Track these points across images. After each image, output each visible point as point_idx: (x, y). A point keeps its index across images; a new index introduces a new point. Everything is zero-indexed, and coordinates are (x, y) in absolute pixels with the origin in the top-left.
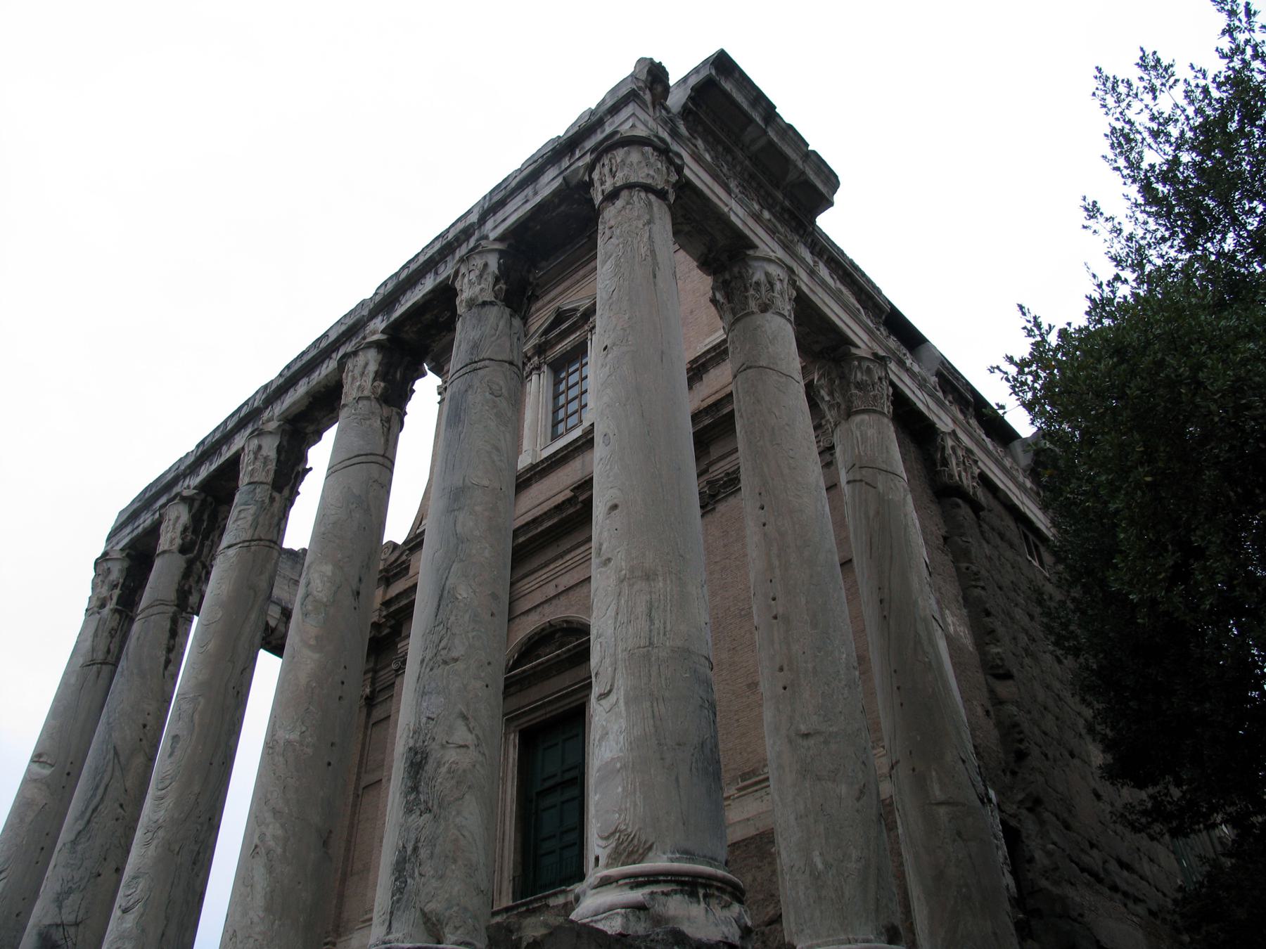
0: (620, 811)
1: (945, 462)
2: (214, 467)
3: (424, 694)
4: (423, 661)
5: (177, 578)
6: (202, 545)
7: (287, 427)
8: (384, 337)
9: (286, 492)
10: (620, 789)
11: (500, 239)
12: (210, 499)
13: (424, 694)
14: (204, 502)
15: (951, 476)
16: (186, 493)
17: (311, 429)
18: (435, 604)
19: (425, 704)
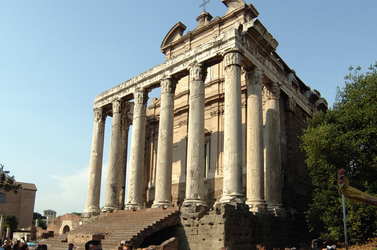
0: (229, 187)
1: (289, 105)
2: (125, 95)
3: (192, 162)
4: (192, 156)
5: (120, 119)
6: (123, 110)
7: (145, 90)
8: (171, 77)
9: (145, 104)
10: (229, 184)
11: (201, 63)
12: (123, 100)
13: (192, 162)
14: (122, 101)
15: (289, 108)
16: (119, 99)
17: (150, 90)
18: (193, 146)
19: (193, 163)
